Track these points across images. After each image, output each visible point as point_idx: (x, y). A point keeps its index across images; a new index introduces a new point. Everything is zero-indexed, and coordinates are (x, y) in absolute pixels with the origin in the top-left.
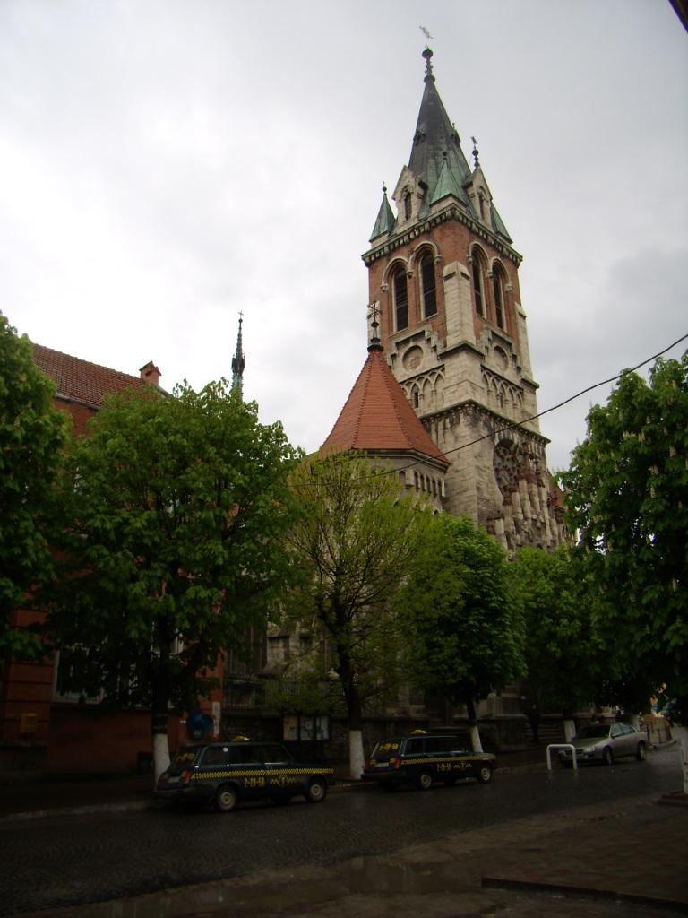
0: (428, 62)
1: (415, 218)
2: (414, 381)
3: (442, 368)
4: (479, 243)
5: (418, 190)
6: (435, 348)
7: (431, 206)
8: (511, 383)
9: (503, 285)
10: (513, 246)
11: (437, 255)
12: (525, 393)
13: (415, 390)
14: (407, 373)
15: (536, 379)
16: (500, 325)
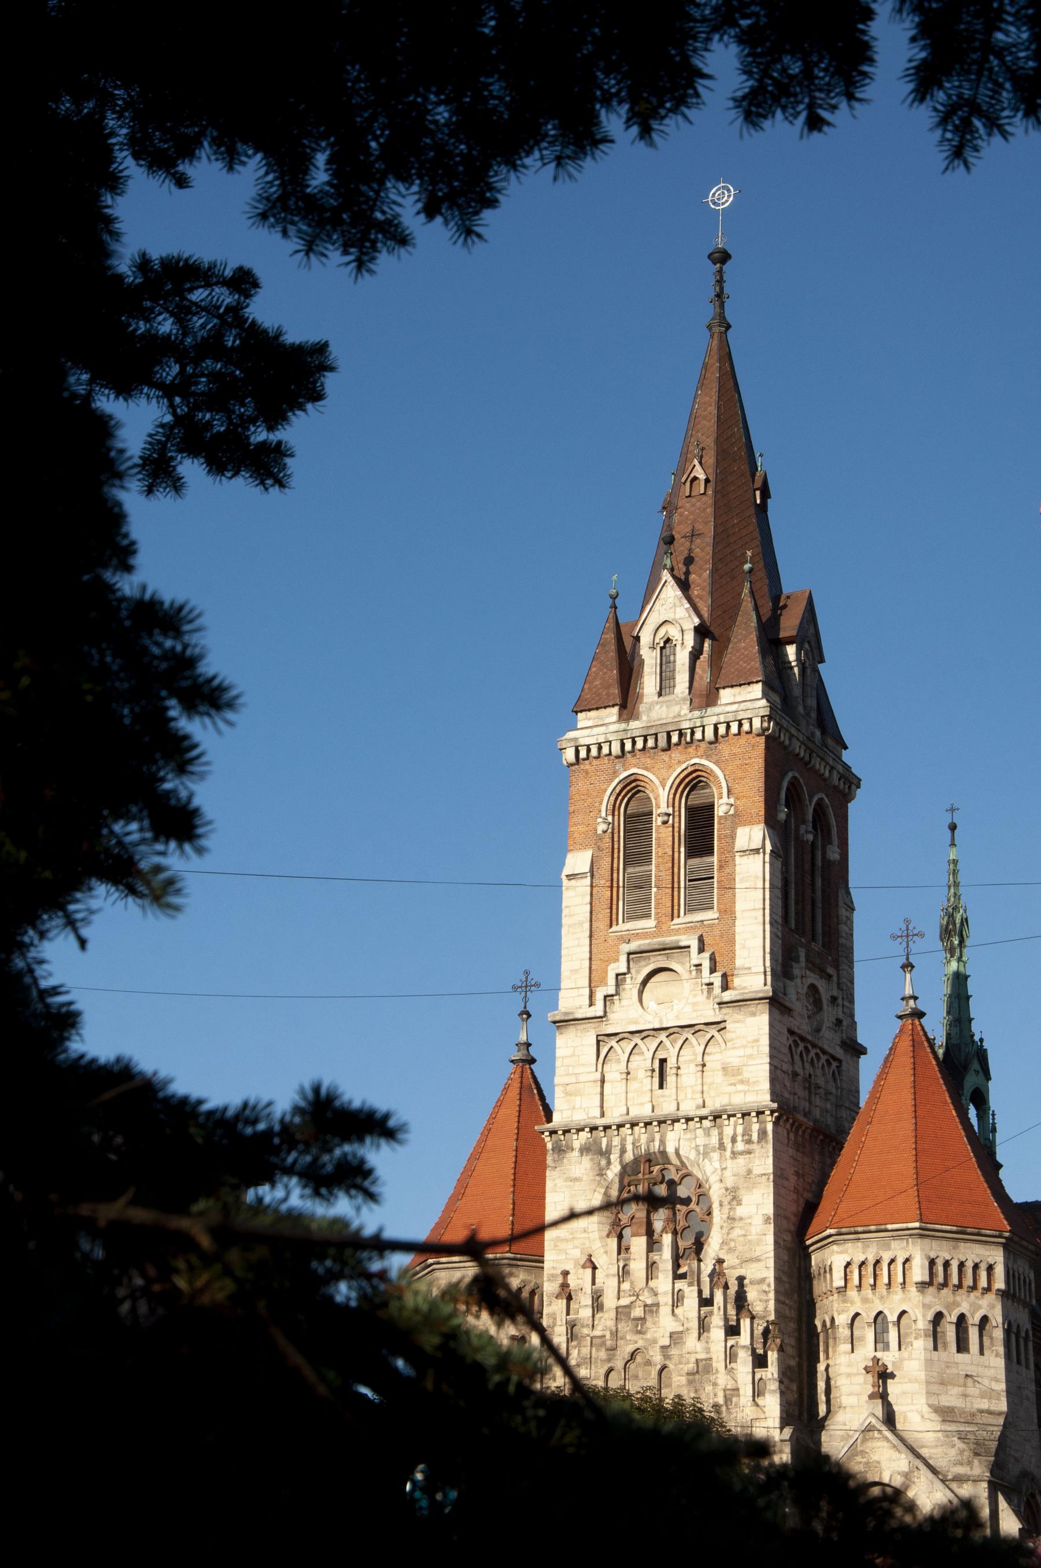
0: (720, 282)
1: (684, 699)
2: (663, 1036)
3: (719, 1025)
4: (797, 775)
5: (690, 640)
6: (712, 984)
7: (718, 689)
8: (824, 1052)
9: (824, 854)
10: (846, 756)
11: (725, 800)
12: (844, 1067)
13: (661, 1055)
14: (650, 1018)
15: (861, 1039)
16: (814, 939)
